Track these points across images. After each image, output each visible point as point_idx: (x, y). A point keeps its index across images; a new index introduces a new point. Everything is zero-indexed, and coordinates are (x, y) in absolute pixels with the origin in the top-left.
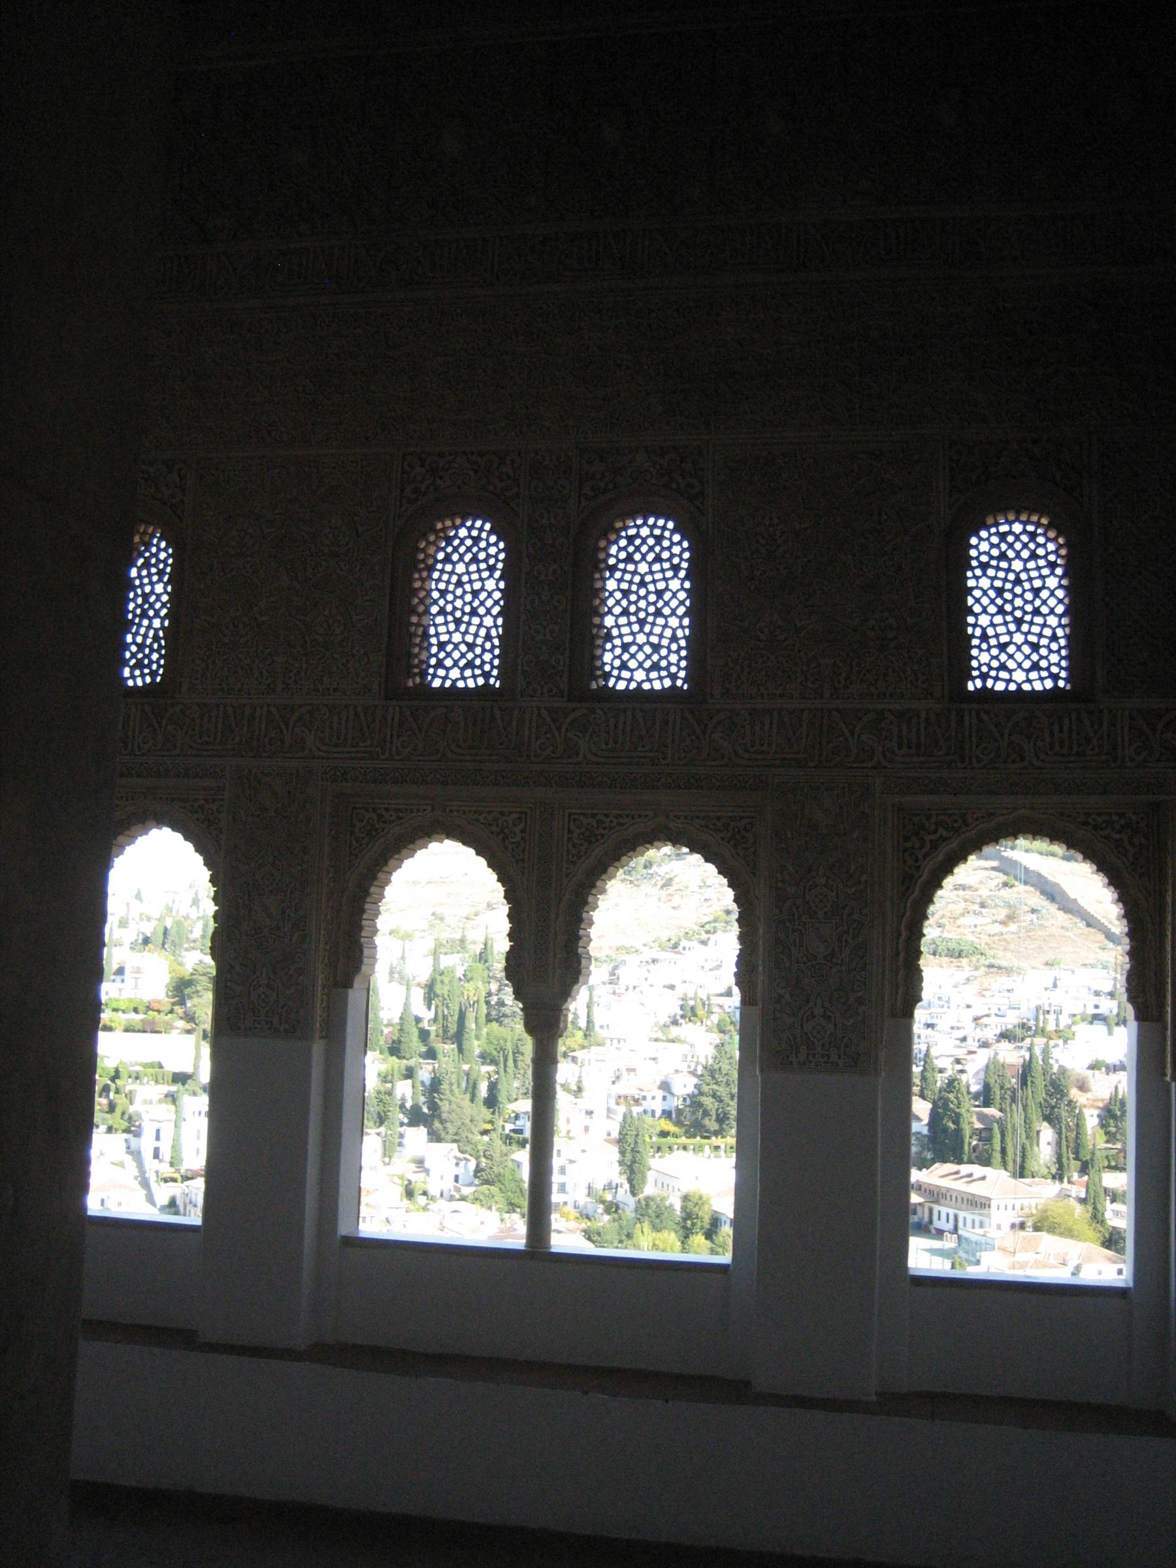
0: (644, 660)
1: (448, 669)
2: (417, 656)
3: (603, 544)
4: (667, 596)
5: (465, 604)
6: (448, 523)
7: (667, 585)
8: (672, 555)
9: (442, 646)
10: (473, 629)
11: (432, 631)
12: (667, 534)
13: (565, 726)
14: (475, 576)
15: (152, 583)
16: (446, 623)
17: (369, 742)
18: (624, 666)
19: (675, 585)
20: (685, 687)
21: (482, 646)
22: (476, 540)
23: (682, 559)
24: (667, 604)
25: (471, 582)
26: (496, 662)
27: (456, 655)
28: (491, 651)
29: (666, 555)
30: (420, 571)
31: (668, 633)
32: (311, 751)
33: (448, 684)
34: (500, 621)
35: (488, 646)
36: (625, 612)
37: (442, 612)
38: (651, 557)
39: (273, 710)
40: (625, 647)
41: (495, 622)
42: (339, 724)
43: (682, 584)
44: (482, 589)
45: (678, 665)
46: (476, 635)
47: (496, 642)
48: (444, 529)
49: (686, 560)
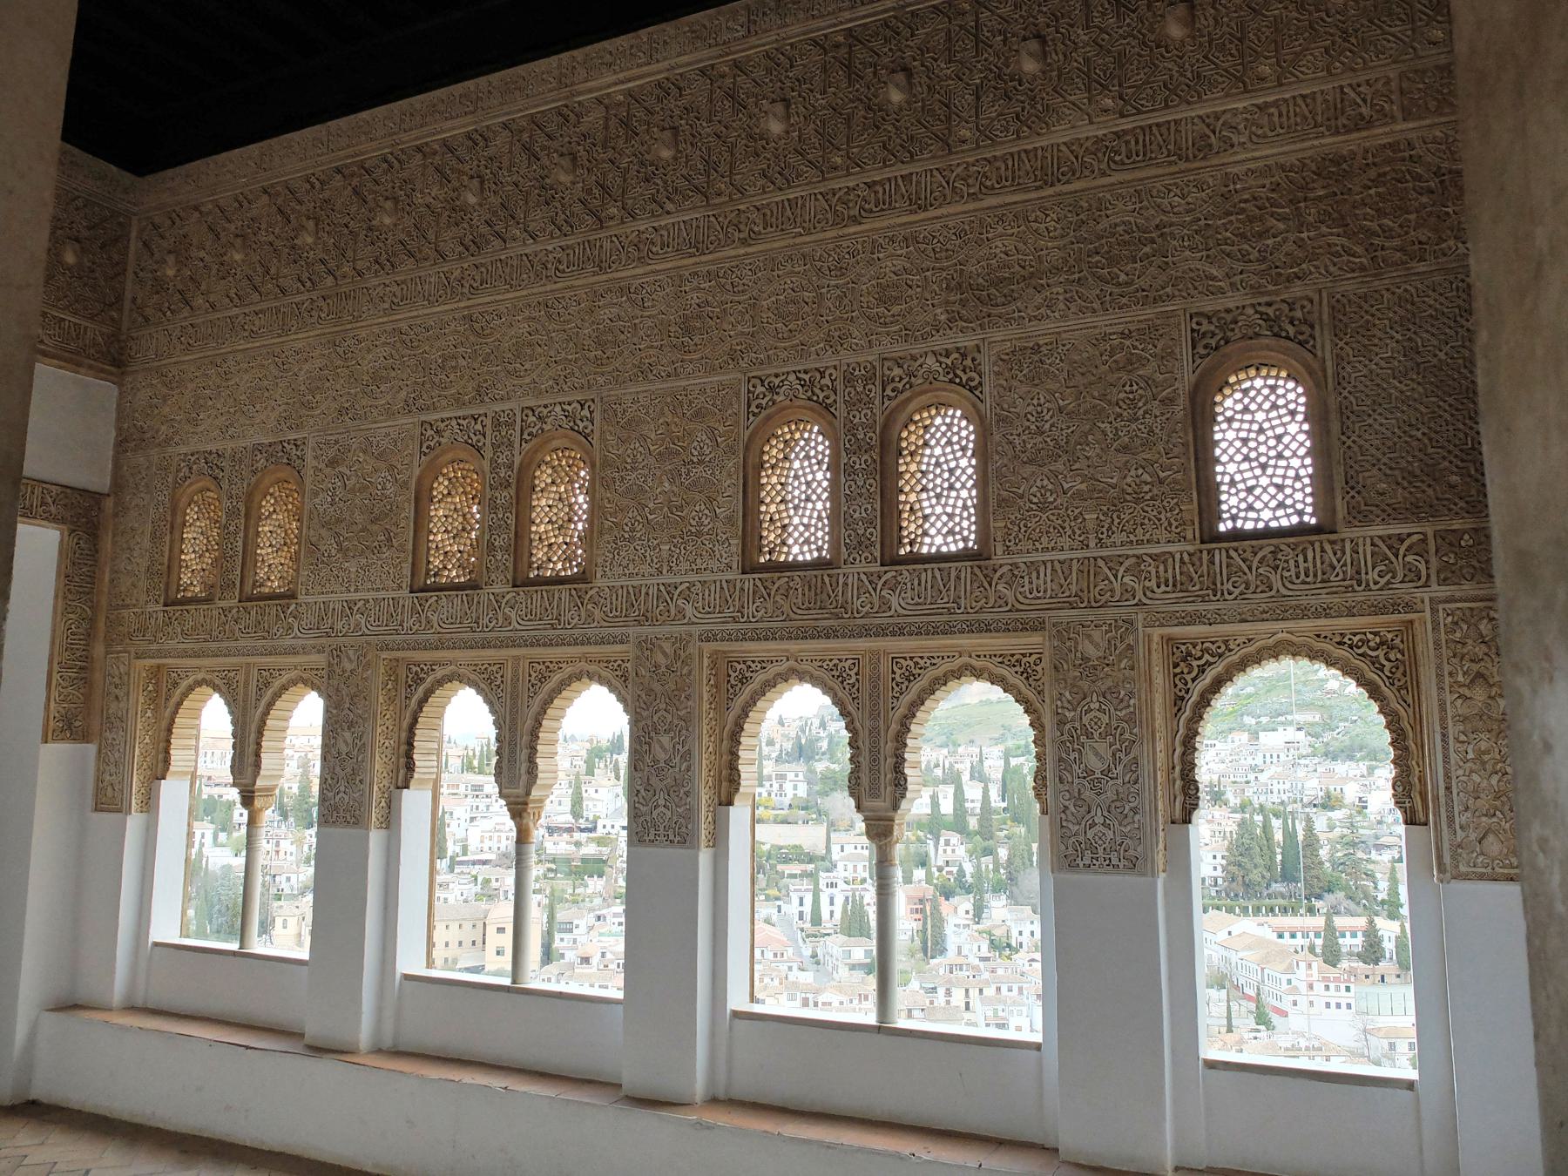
14: (950, 457)
15: (813, 473)
16: (929, 499)
22: (950, 426)
25: (947, 462)
30: (904, 457)
35: (965, 514)
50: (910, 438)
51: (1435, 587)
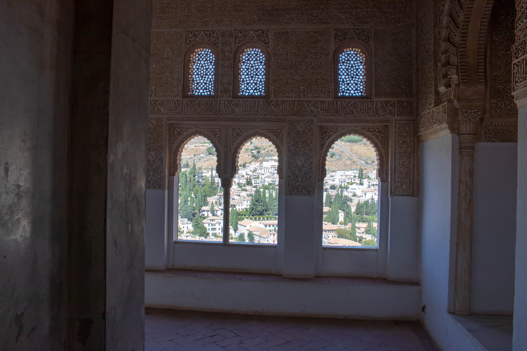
0: (253, 87)
1: (200, 90)
2: (191, 86)
3: (241, 56)
4: (259, 70)
5: (204, 72)
6: (199, 50)
7: (259, 67)
8: (260, 59)
9: (198, 83)
10: (206, 79)
11: (195, 79)
12: (259, 53)
13: (232, 105)
17: (332, 112)
18: (247, 89)
19: (261, 67)
20: (264, 94)
21: (209, 84)
22: (207, 55)
23: (263, 60)
24: (259, 72)
25: (205, 66)
26: (213, 88)
27: (202, 86)
28: (211, 85)
29: (258, 59)
31: (259, 80)
32: (355, 114)
33: (200, 94)
34: (213, 77)
36: (248, 74)
37: (198, 74)
38: (254, 59)
39: (152, 101)
40: (248, 84)
41: (212, 77)
42: (170, 105)
43: (263, 67)
44: (209, 68)
45: (262, 89)
46: (207, 81)
47: (213, 82)
48: (198, 52)
49: (264, 60)
50: (194, 57)
51: (396, 116)
